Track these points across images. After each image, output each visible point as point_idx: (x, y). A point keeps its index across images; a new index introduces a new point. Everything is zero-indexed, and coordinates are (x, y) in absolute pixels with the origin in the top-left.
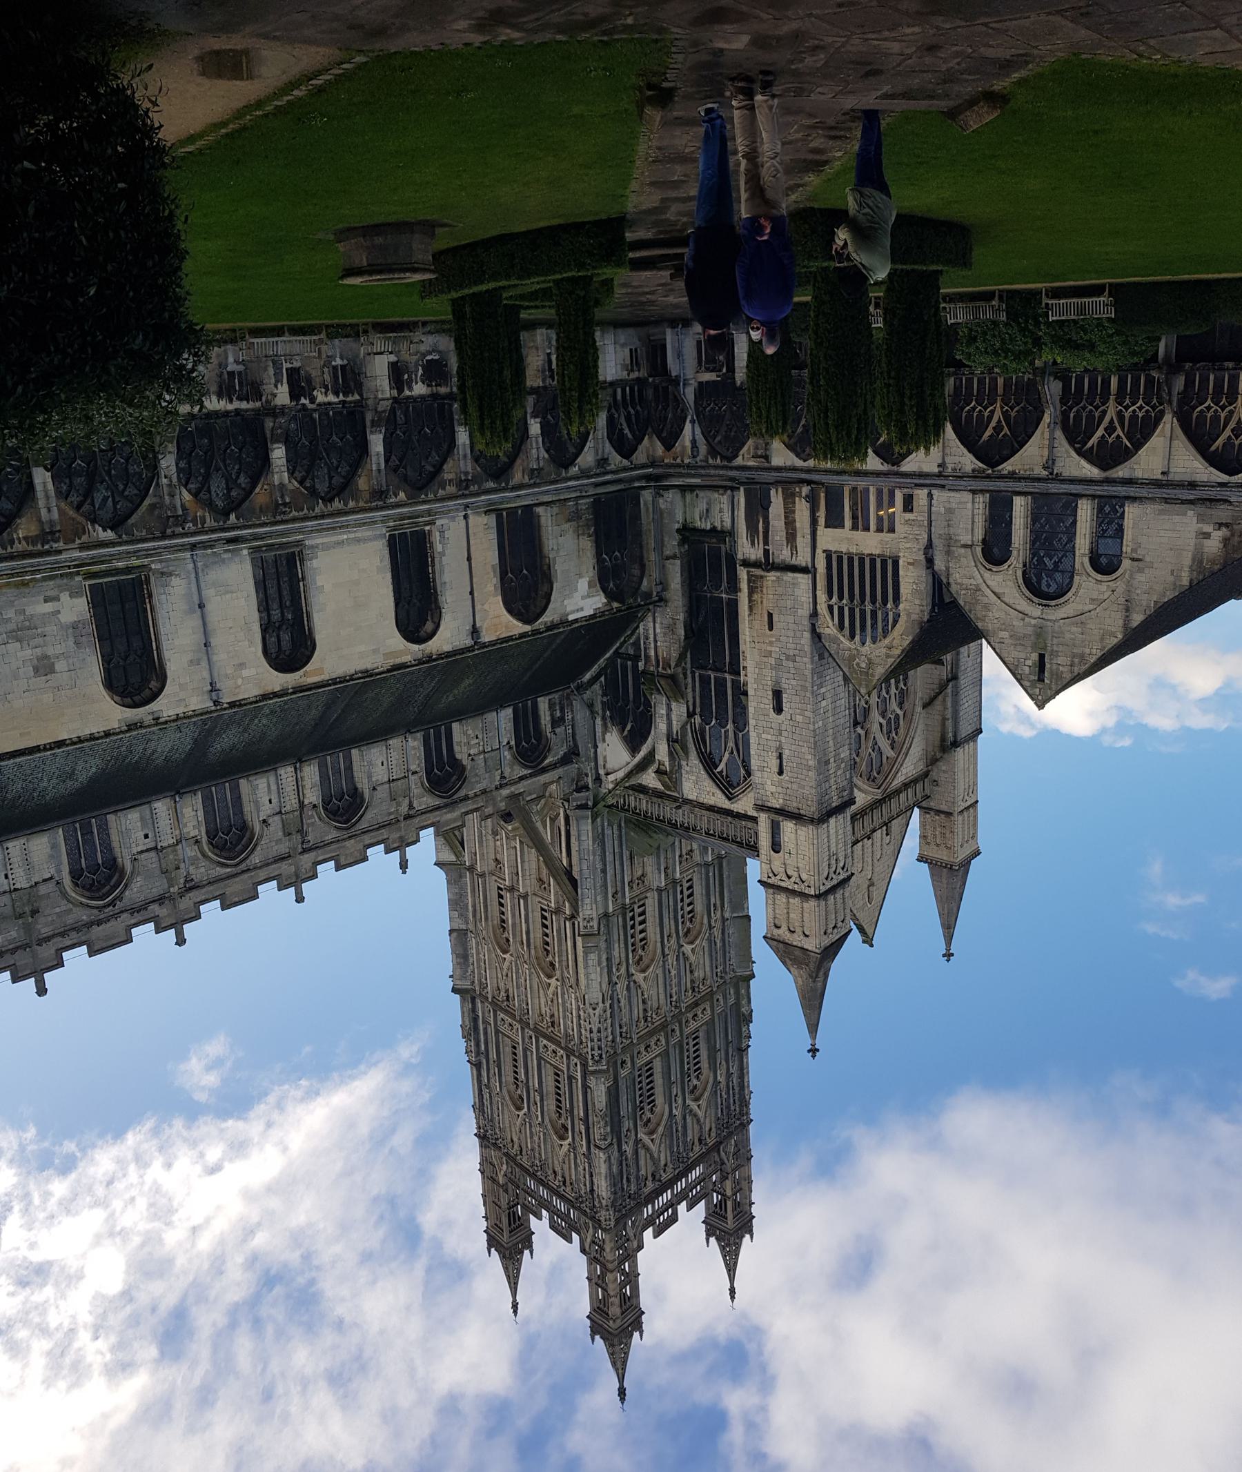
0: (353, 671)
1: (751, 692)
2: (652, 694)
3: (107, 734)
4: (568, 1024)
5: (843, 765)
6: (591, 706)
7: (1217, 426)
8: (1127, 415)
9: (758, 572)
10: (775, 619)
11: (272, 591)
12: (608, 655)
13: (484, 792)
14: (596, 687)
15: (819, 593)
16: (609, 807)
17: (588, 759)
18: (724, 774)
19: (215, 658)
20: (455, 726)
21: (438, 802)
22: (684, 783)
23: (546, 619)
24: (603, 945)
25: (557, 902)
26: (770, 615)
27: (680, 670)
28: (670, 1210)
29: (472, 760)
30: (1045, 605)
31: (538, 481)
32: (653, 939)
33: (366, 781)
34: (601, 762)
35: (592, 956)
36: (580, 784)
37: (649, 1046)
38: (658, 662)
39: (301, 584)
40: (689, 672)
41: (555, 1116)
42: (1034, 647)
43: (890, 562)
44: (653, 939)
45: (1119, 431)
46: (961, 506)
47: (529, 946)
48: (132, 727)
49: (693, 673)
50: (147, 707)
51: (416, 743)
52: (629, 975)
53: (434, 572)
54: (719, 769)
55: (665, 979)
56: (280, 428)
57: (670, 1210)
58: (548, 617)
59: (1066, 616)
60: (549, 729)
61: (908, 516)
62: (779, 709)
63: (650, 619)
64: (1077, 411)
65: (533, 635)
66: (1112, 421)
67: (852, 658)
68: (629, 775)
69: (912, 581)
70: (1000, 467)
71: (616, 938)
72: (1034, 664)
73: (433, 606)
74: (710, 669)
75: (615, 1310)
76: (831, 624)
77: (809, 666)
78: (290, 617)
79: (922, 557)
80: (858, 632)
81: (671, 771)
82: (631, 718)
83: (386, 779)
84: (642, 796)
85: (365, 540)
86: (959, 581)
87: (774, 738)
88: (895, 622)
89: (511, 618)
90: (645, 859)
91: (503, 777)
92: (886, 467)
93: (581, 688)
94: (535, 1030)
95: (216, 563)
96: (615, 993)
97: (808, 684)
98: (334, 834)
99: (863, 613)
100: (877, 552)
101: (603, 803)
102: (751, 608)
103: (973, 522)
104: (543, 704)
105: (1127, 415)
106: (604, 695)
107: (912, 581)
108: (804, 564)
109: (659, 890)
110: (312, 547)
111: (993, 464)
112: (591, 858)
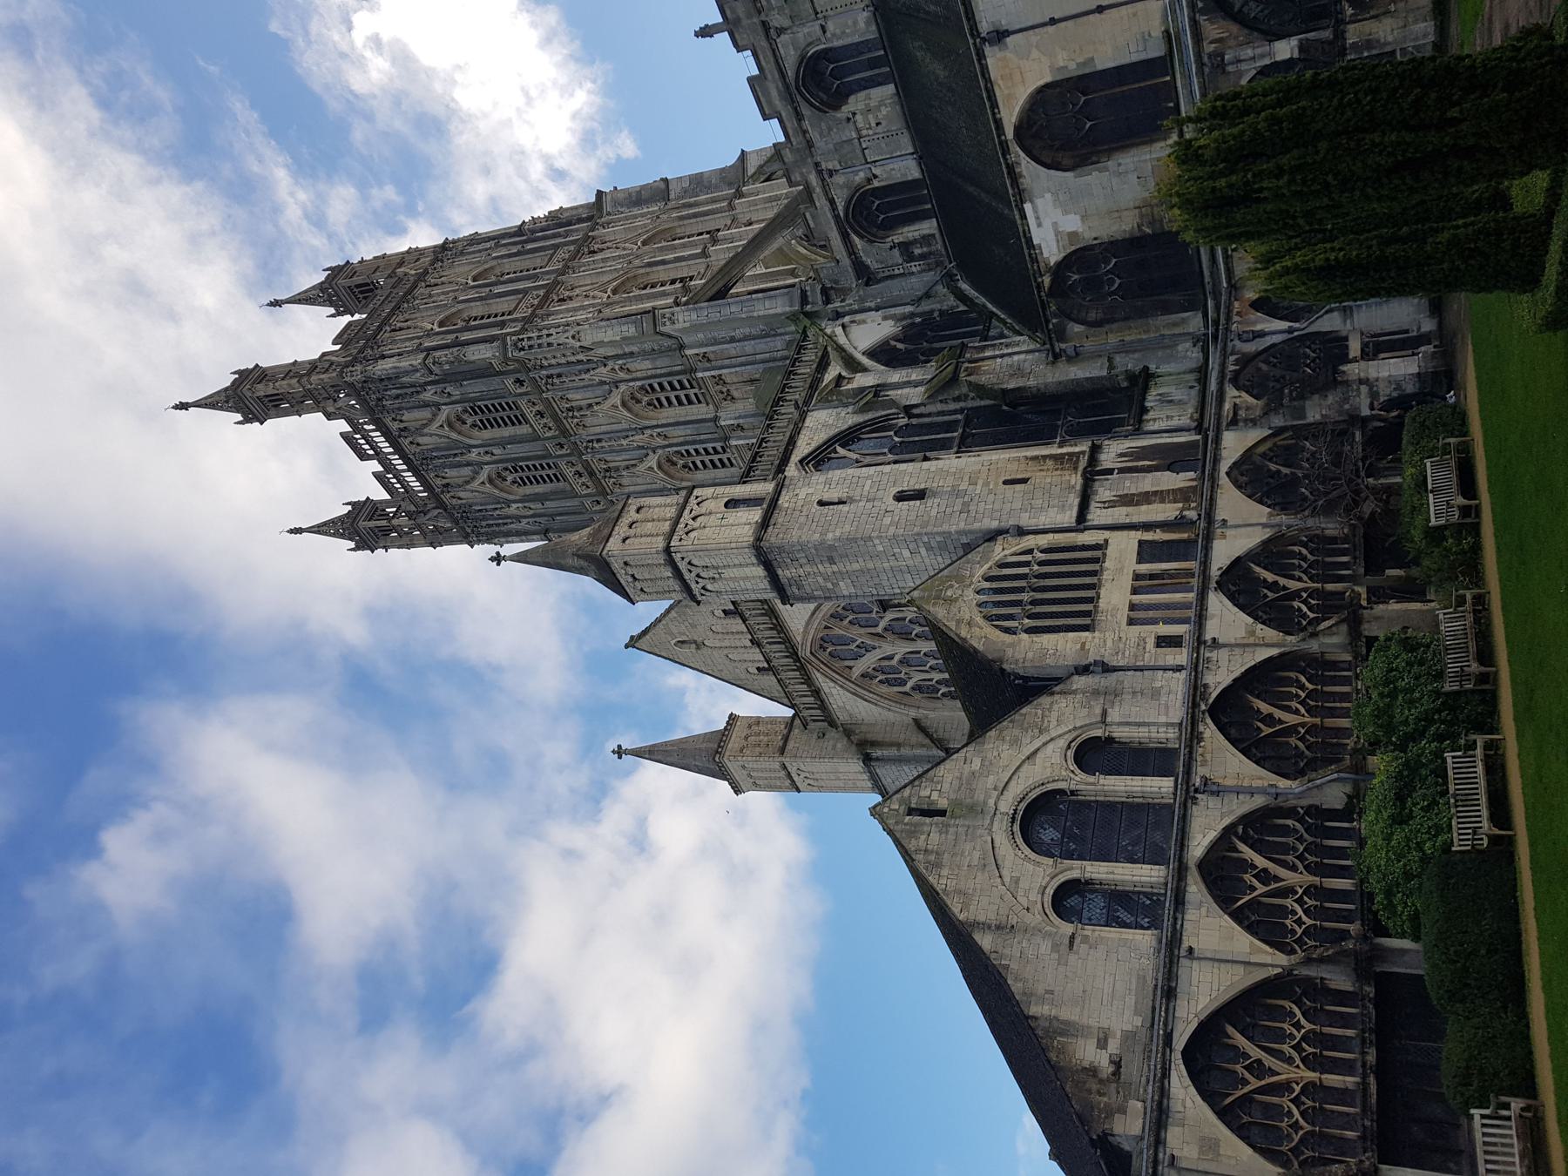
1: (926, 464)
2: (937, 362)
4: (560, 314)
5: (830, 585)
6: (927, 295)
7: (1268, 1038)
8: (1289, 902)
9: (1083, 463)
10: (1018, 487)
12: (989, 306)
13: (810, 144)
14: (952, 301)
15: (1050, 536)
16: (804, 332)
17: (862, 300)
18: (833, 455)
20: (890, 88)
21: (791, 74)
22: (826, 411)
23: (1024, 163)
24: (647, 346)
26: (1024, 481)
27: (965, 390)
28: (371, 452)
29: (849, 119)
30: (1013, 819)
31: (1207, 70)
32: (660, 416)
34: (858, 317)
35: (632, 330)
36: (832, 292)
37: (543, 417)
38: (976, 361)
40: (962, 404)
41: (465, 316)
42: (956, 803)
43: (1087, 621)
44: (660, 416)
45: (1261, 889)
46: (1162, 707)
47: (650, 265)
49: (961, 411)
51: (862, 25)
52: (616, 384)
54: (839, 449)
55: (617, 432)
57: (371, 452)
58: (1028, 168)
59: (997, 844)
60: (897, 239)
61: (1151, 642)
62: (901, 497)
63: (1032, 347)
64: (1296, 831)
65: (1001, 143)
66: (1277, 879)
67: (960, 579)
68: (840, 349)
69: (1061, 648)
70: (1209, 721)
71: (659, 363)
72: (933, 803)
74: (964, 431)
75: (262, 390)
76: (1006, 552)
77: (953, 529)
79: (1091, 660)
80: (995, 585)
81: (840, 393)
82: (912, 347)
84: (815, 366)
86: (1055, 707)
87: (865, 493)
88: (1007, 630)
89: (1021, 102)
90: (751, 400)
91: (831, 173)
92: (1215, 572)
93: (949, 279)
94: (556, 283)
96: (595, 365)
97: (929, 529)
99: (1021, 590)
100: (1102, 604)
101: (807, 322)
102: (1035, 458)
103: (1139, 725)
104: (928, 227)
105: (1289, 902)
106: (942, 313)
107: (1061, 648)
108: (1089, 517)
109: (715, 419)
111: (1216, 712)
112: (743, 316)
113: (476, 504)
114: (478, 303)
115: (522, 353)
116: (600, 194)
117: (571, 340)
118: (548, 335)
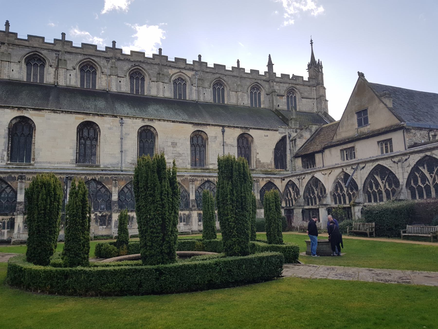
0: (61, 114)
3: (160, 120)
11: (88, 151)
19: (120, 134)
33: (23, 67)
39: (78, 151)
48: (152, 120)
53: (9, 143)
56: (116, 206)
73: (11, 129)
78: (82, 141)
83: (11, 63)
85: (46, 162)
95: (114, 165)
98: (44, 52)
110: (72, 164)
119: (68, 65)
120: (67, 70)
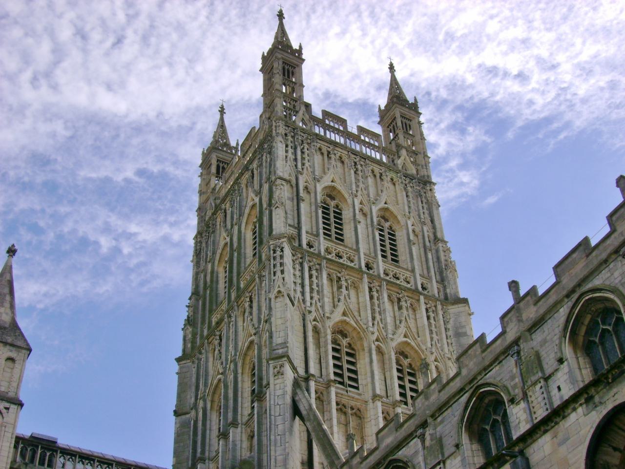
21: (401, 454)
25: (329, 393)
35: (280, 341)
41: (342, 205)
50: (605, 412)
83: (448, 462)
90: (248, 454)
98: (492, 376)
109: (234, 424)
112: (272, 437)
113: (215, 237)
114: (351, 214)
115: (272, 252)
116: (465, 301)
117: (276, 290)
118: (282, 272)
119: (545, 366)
120: (546, 379)
